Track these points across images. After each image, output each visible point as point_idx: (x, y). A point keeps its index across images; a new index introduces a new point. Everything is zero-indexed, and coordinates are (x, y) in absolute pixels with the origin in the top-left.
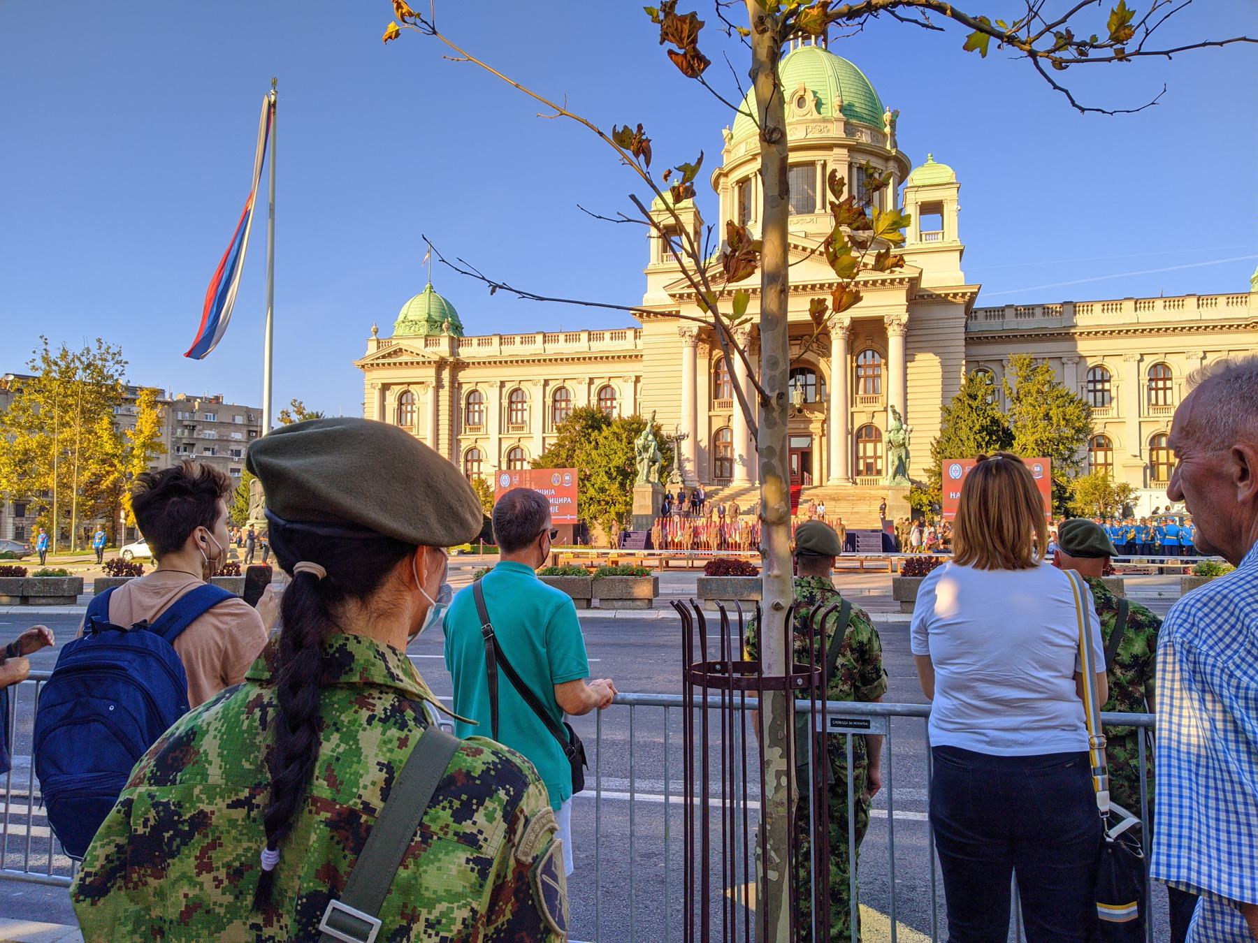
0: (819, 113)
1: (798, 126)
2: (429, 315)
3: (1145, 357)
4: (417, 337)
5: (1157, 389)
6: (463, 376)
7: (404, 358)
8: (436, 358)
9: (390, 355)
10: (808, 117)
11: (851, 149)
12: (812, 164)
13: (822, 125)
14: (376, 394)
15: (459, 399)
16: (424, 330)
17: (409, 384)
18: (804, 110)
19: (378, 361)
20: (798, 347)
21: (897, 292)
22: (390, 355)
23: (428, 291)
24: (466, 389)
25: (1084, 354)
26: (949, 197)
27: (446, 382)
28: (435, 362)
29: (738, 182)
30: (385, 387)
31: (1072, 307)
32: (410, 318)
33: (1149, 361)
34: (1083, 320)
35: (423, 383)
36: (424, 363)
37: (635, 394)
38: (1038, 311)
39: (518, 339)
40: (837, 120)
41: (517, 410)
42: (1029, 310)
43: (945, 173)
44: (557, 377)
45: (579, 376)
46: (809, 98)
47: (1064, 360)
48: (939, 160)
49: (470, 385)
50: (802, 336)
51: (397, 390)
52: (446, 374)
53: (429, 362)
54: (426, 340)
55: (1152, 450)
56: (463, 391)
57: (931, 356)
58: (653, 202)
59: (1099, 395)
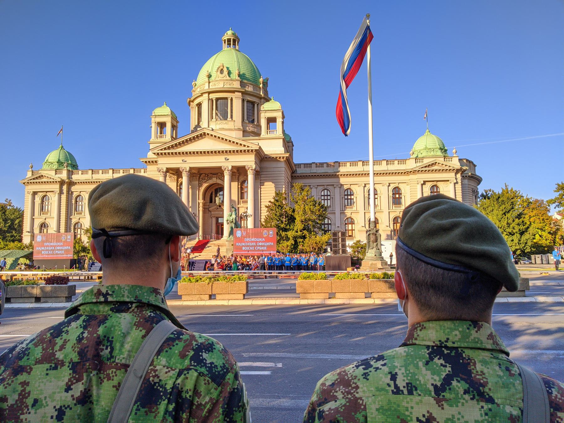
0: (230, 77)
1: (221, 82)
2: (59, 160)
3: (391, 184)
4: (51, 170)
5: (348, 199)
6: (73, 188)
7: (44, 180)
8: (59, 180)
9: (37, 178)
10: (225, 78)
11: (243, 93)
12: (226, 99)
13: (231, 82)
15: (71, 199)
16: (56, 166)
17: (47, 192)
18: (223, 75)
19: (31, 181)
21: (251, 155)
22: (37, 178)
23: (60, 149)
24: (75, 195)
25: (343, 183)
26: (278, 115)
28: (59, 182)
29: (197, 105)
30: (35, 193)
31: (338, 164)
32: (50, 161)
34: (342, 170)
35: (53, 191)
36: (53, 182)
38: (325, 165)
39: (101, 172)
40: (237, 80)
42: (322, 165)
46: (225, 70)
47: (335, 186)
49: (77, 193)
51: (41, 195)
52: (65, 188)
53: (56, 182)
54: (56, 171)
55: (394, 223)
56: (73, 196)
57: (271, 183)
58: (153, 112)
59: (349, 201)
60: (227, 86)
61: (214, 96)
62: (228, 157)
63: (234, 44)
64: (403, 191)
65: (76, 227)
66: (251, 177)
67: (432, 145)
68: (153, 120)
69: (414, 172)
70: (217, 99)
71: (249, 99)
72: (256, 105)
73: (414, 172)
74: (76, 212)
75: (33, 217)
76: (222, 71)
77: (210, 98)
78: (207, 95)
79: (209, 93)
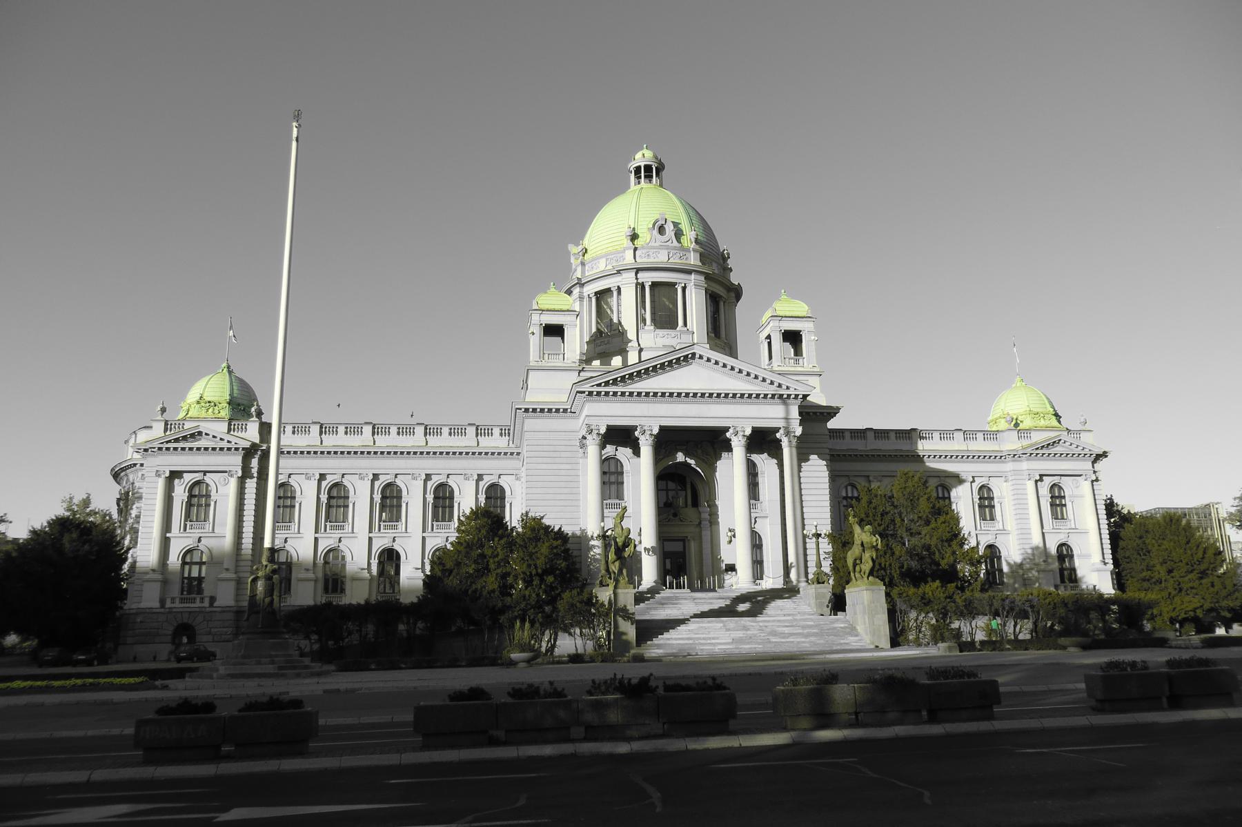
0: (679, 241)
7: (203, 443)
9: (185, 438)
12: (673, 285)
14: (161, 484)
16: (225, 413)
17: (205, 473)
19: (169, 445)
27: (255, 471)
28: (243, 449)
29: (596, 293)
30: (175, 475)
32: (208, 399)
36: (229, 449)
41: (199, 505)
43: (801, 308)
44: (511, 472)
45: (414, 471)
46: (669, 228)
48: (794, 295)
53: (237, 449)
54: (230, 425)
60: (676, 261)
61: (648, 278)
64: (996, 494)
65: (188, 559)
67: (1037, 406)
68: (536, 318)
70: (654, 285)
72: (721, 304)
74: (328, 524)
75: (168, 535)
76: (661, 230)
77: (640, 281)
79: (638, 270)
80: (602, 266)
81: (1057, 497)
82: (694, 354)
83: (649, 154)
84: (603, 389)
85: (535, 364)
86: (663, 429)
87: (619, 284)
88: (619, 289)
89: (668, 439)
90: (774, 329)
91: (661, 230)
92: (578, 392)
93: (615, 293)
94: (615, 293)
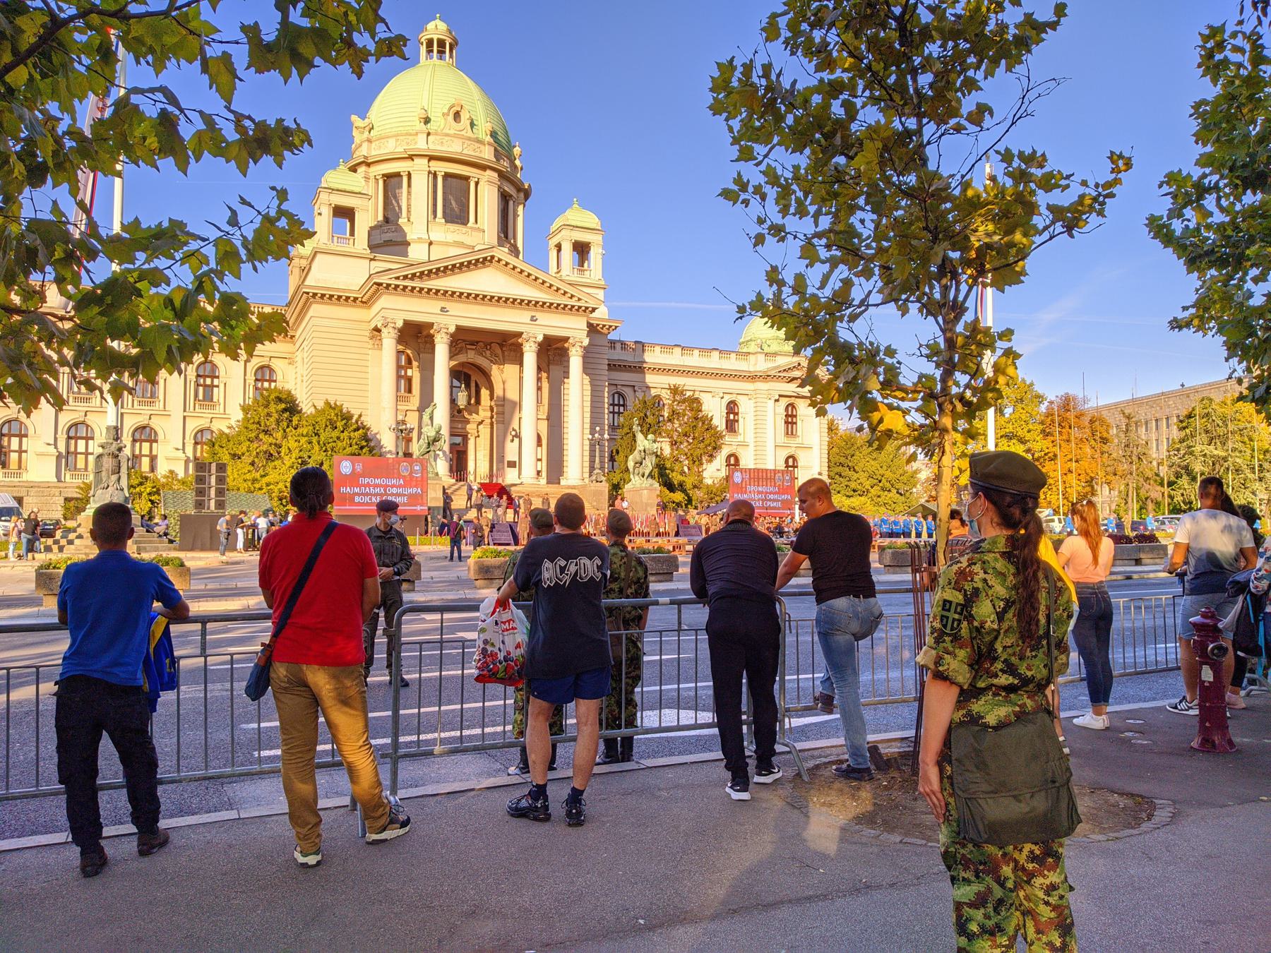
1: (455, 140)
10: (463, 133)
12: (467, 178)
13: (477, 145)
20: (473, 352)
25: (651, 385)
29: (384, 175)
31: (641, 345)
33: (727, 398)
37: (245, 375)
38: (618, 346)
43: (592, 220)
48: (585, 206)
50: (477, 342)
60: (469, 152)
61: (442, 168)
62: (538, 315)
63: (441, 52)
66: (575, 363)
68: (324, 197)
69: (766, 377)
70: (447, 176)
71: (506, 189)
72: (511, 203)
73: (766, 377)
76: (457, 116)
77: (432, 169)
78: (425, 161)
79: (431, 158)
80: (390, 147)
81: (791, 416)
82: (493, 257)
83: (442, 26)
84: (402, 283)
85: (324, 247)
86: (460, 329)
87: (410, 169)
88: (409, 175)
89: (463, 339)
90: (567, 239)
91: (457, 116)
92: (375, 283)
93: (405, 179)
94: (405, 179)
